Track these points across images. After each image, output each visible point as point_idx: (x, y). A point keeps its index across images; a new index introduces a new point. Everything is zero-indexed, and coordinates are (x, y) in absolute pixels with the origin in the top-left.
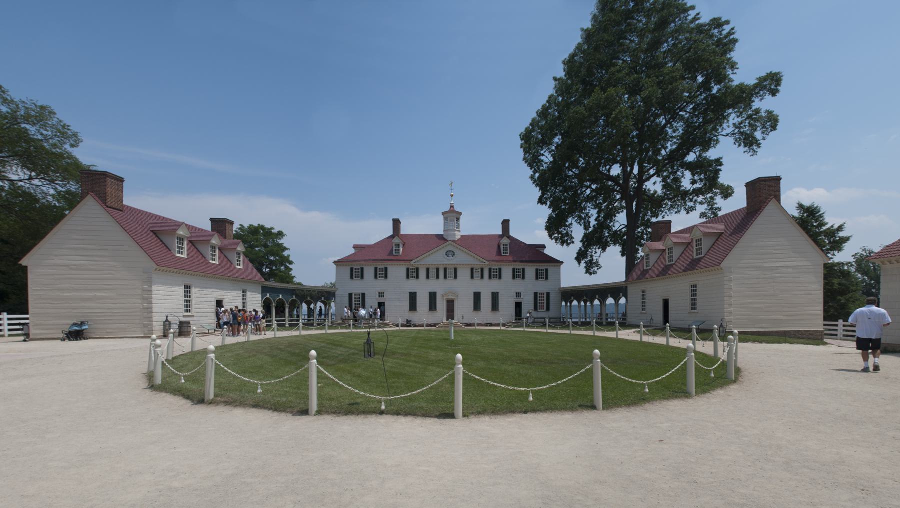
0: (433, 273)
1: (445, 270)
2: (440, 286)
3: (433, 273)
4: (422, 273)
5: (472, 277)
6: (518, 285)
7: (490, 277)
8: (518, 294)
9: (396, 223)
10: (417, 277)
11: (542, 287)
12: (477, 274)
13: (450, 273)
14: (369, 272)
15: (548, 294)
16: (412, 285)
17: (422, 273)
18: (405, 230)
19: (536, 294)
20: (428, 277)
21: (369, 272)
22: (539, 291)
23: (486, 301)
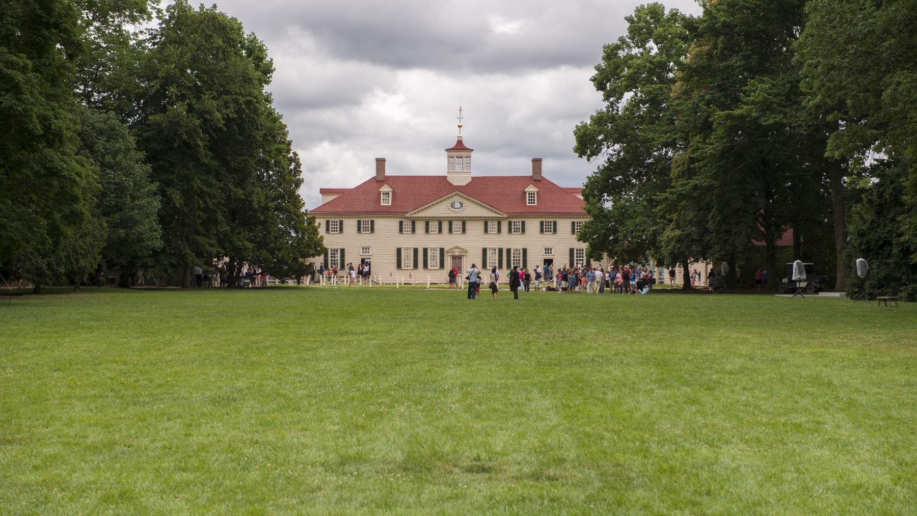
1: (450, 224)
3: (434, 226)
4: (420, 226)
5: (486, 231)
6: (548, 239)
7: (510, 231)
9: (381, 163)
10: (413, 231)
13: (457, 225)
14: (350, 224)
17: (420, 226)
20: (427, 231)
21: (350, 224)
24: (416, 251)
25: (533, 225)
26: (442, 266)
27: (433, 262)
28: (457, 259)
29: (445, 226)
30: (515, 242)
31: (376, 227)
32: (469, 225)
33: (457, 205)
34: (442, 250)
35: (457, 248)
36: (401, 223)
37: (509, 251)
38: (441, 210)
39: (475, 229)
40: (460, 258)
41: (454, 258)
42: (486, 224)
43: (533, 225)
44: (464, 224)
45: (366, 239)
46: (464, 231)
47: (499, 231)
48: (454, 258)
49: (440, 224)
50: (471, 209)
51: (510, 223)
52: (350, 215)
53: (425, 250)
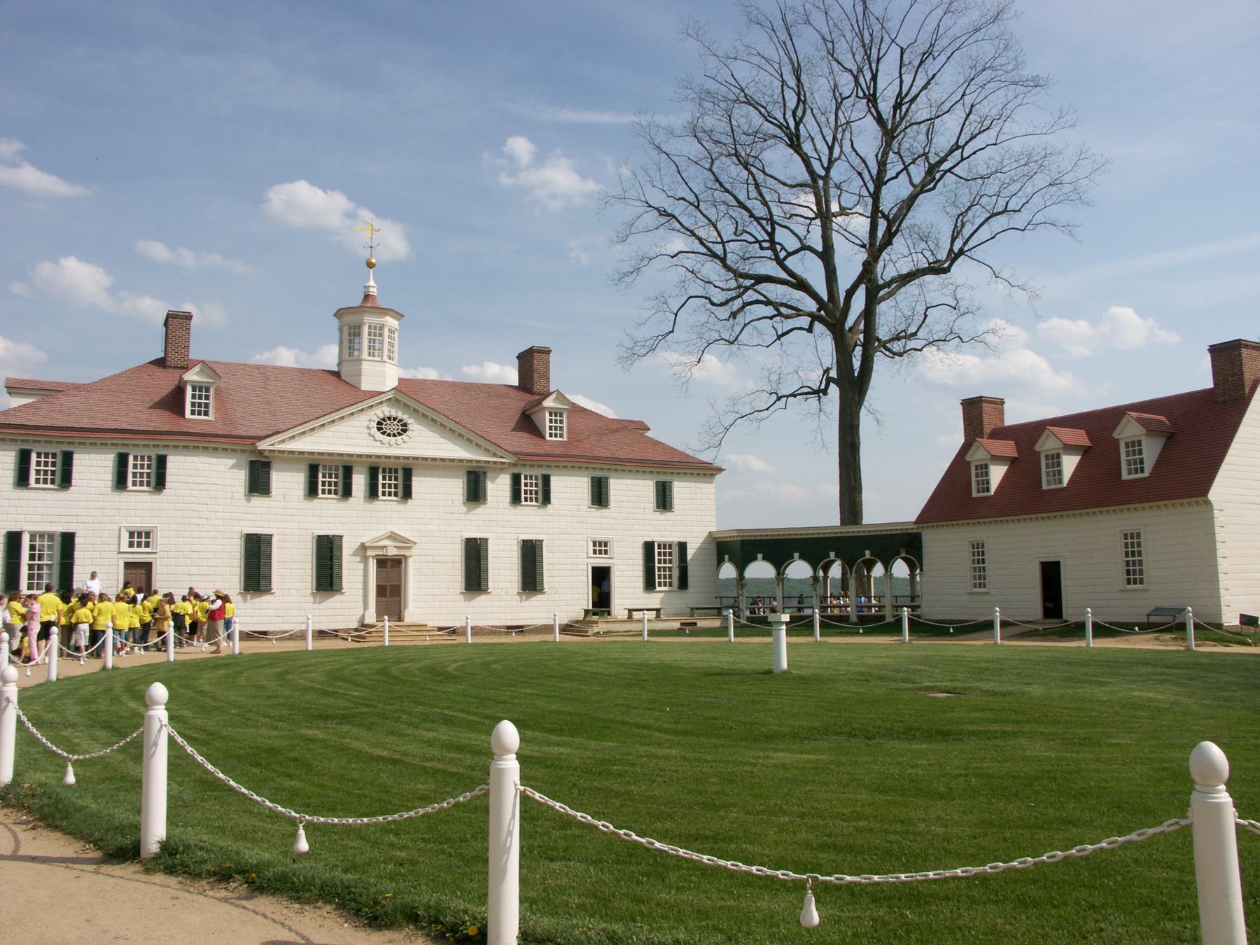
1: (373, 473)
2: (360, 522)
8: (601, 547)
11: (666, 529)
15: (683, 547)
16: (259, 516)
19: (649, 547)
22: (657, 538)
23: (503, 567)
29: (359, 481)
32: (418, 483)
35: (393, 536)
38: (350, 436)
43: (570, 488)
44: (408, 474)
45: (139, 506)
50: (422, 442)
52: (95, 436)
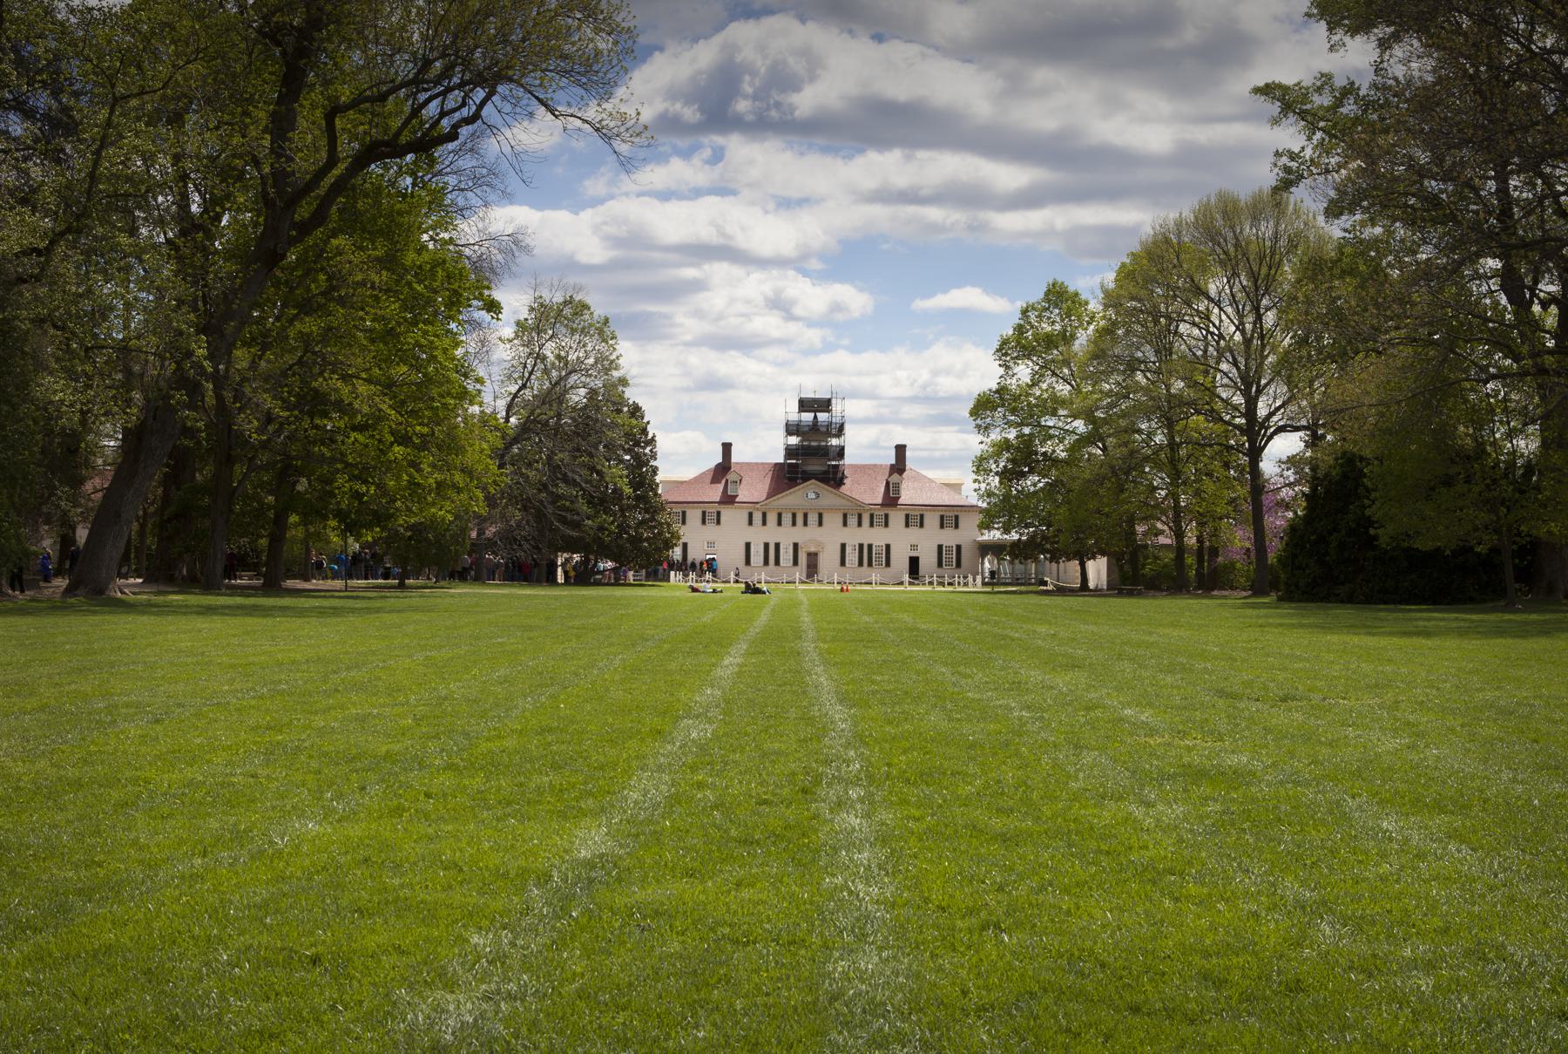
0: (787, 518)
1: (805, 516)
3: (787, 518)
5: (845, 524)
6: (914, 534)
7: (872, 525)
8: (914, 547)
9: (727, 448)
12: (853, 521)
13: (813, 518)
15: (959, 547)
18: (736, 457)
19: (940, 547)
24: (766, 546)
25: (897, 518)
26: (796, 563)
27: (786, 556)
28: (813, 559)
30: (877, 537)
31: (723, 519)
33: (811, 495)
34: (796, 546)
36: (751, 515)
37: (870, 546)
39: (832, 520)
40: (816, 554)
41: (809, 554)
42: (845, 516)
44: (820, 516)
45: (711, 531)
46: (820, 524)
47: (860, 524)
48: (809, 554)
49: (794, 516)
51: (872, 516)
53: (777, 546)
